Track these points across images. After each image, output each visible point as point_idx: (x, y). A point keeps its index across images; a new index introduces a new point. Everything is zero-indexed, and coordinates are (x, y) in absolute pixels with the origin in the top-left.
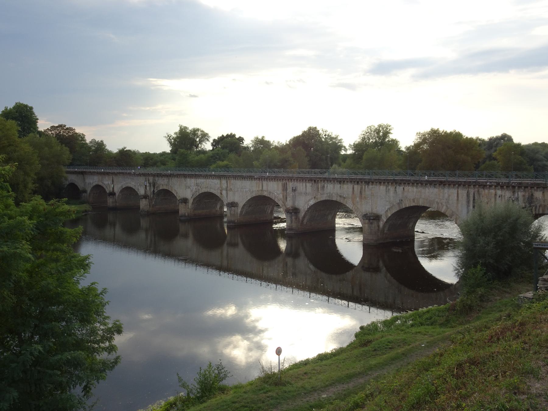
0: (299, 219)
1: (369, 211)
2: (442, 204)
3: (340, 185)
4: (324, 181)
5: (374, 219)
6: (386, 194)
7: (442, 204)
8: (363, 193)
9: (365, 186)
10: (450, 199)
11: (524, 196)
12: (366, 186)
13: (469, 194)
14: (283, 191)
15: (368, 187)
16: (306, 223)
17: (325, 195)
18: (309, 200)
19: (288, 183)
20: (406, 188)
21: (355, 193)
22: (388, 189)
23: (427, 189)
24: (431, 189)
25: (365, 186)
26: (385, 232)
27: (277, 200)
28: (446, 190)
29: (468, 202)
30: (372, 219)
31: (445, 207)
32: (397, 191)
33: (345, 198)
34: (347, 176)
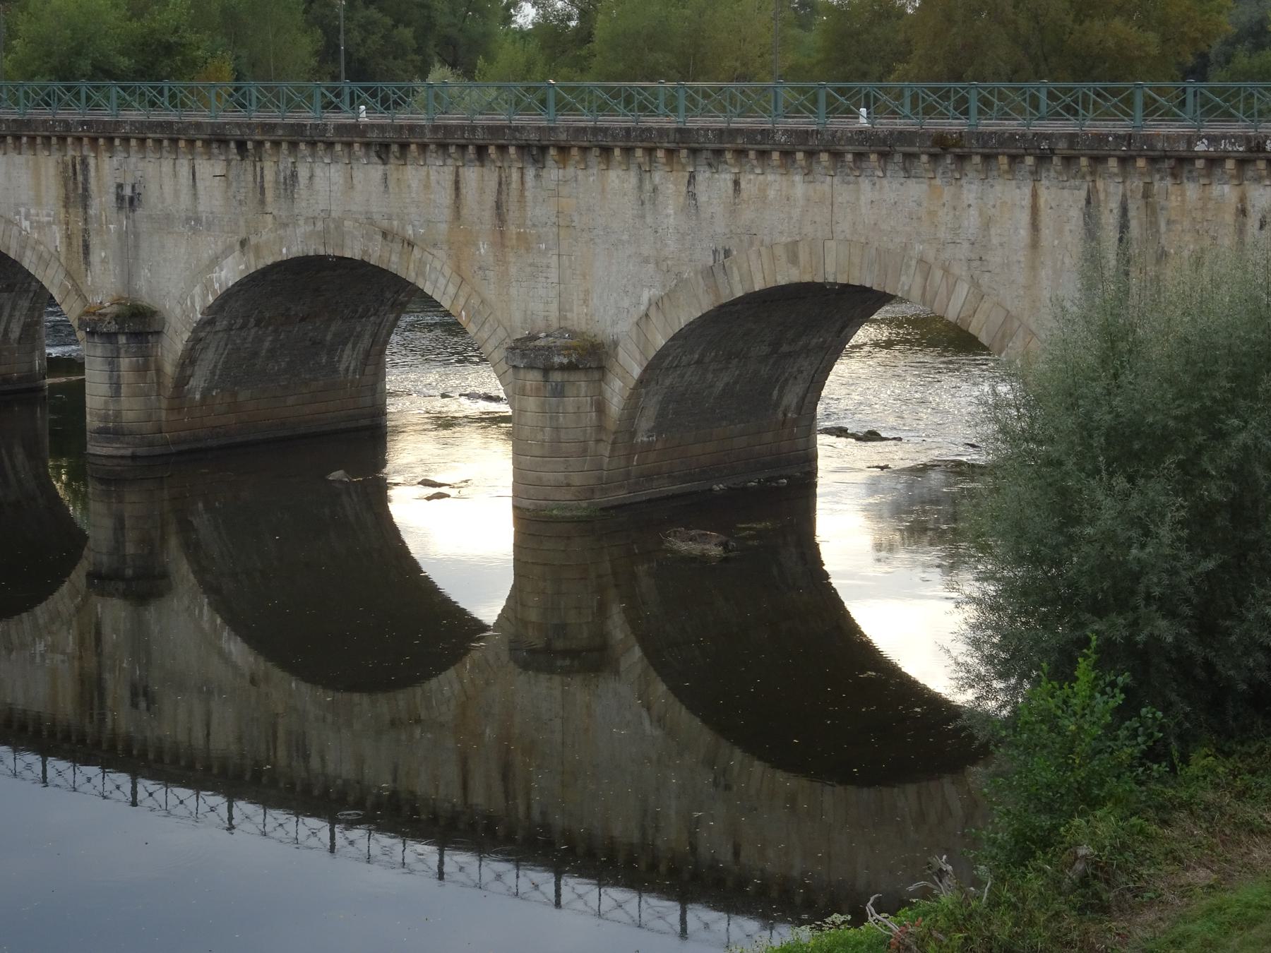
0: (159, 371)
1: (546, 318)
2: (946, 271)
3: (381, 168)
4: (294, 145)
5: (570, 367)
6: (643, 217)
7: (946, 271)
8: (513, 214)
10: (995, 241)
14: (66, 206)
15: (537, 176)
16: (204, 397)
17: (303, 229)
18: (215, 261)
19: (92, 162)
20: (753, 181)
21: (465, 212)
22: (648, 186)
23: (865, 184)
24: (885, 182)
26: (641, 438)
27: (34, 259)
28: (971, 190)
30: (562, 368)
31: (963, 290)
32: (702, 198)
33: (411, 244)
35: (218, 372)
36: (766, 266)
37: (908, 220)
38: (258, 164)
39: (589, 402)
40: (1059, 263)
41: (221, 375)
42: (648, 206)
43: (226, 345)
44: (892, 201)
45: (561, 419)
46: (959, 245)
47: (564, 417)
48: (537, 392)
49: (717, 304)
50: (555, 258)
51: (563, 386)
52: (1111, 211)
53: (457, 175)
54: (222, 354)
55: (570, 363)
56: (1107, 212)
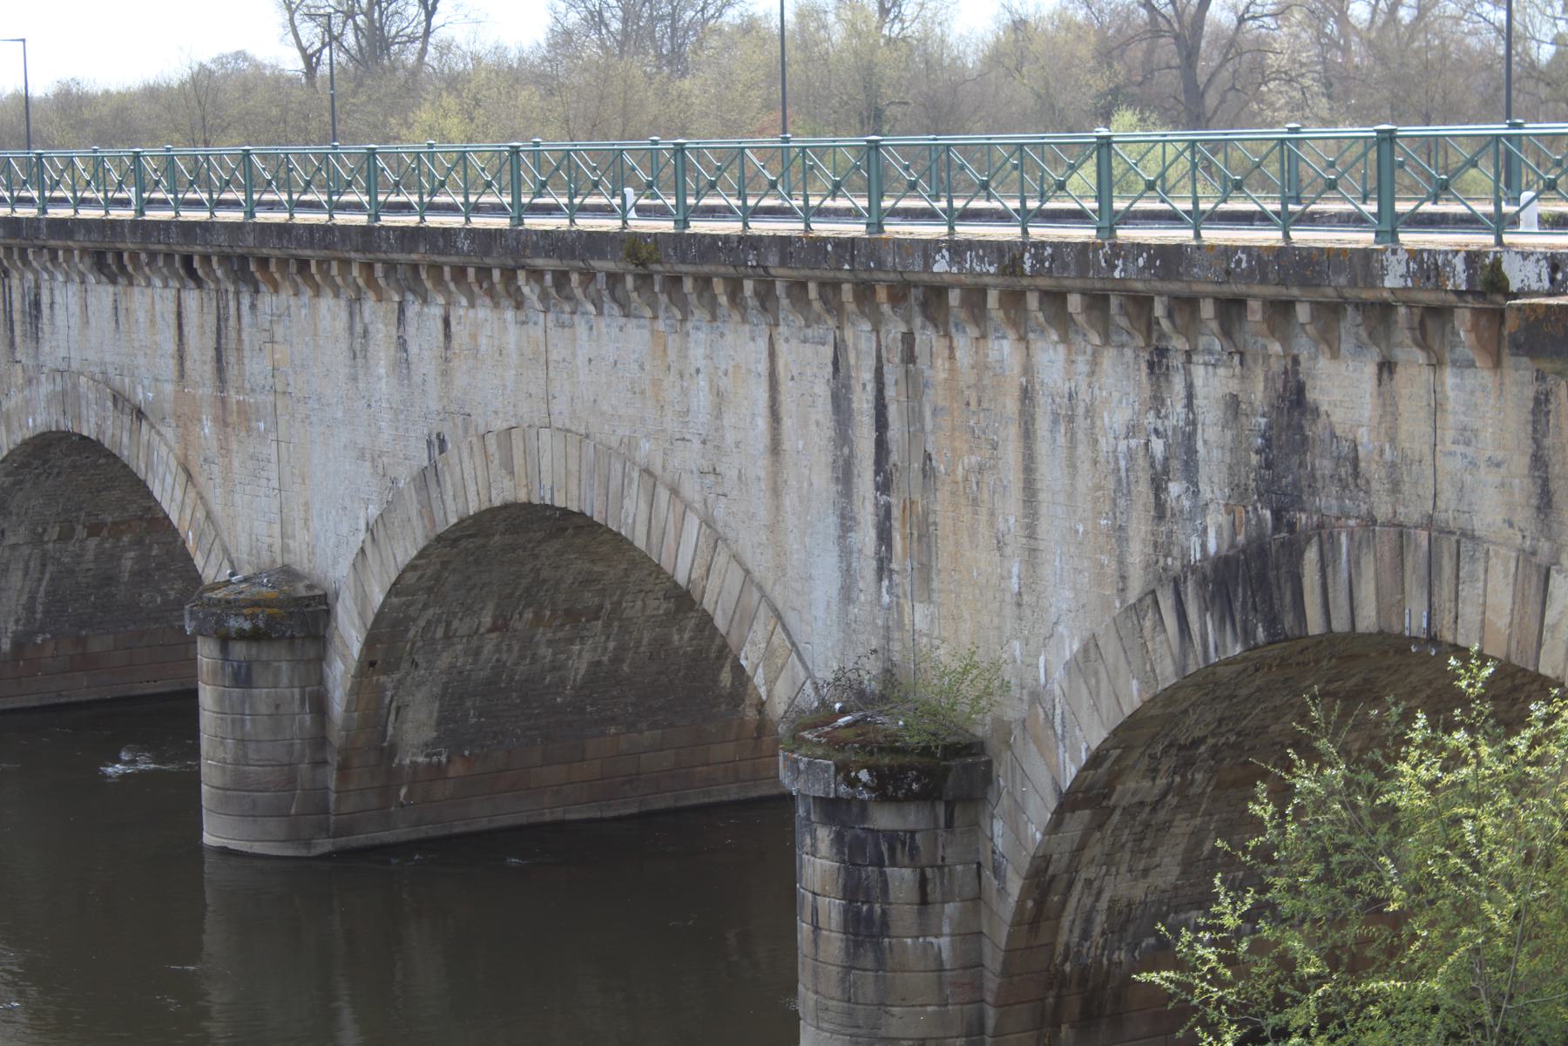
3: (110, 289)
5: (255, 636)
6: (355, 379)
8: (232, 372)
9: (237, 293)
10: (730, 437)
11: (1234, 405)
12: (246, 301)
13: (848, 387)
24: (602, 324)
25: (237, 293)
29: (844, 475)
30: (242, 636)
33: (139, 414)
34: (1357, 220)
35: (40, 608)
36: (479, 473)
37: (630, 395)
38: (6, 281)
39: (297, 696)
40: (805, 484)
41: (46, 612)
42: (360, 361)
43: (44, 566)
44: (612, 360)
45: (248, 725)
46: (688, 444)
47: (253, 721)
49: (432, 536)
50: (274, 444)
51: (249, 669)
52: (864, 386)
53: (179, 298)
54: (40, 580)
55: (255, 628)
56: (858, 388)
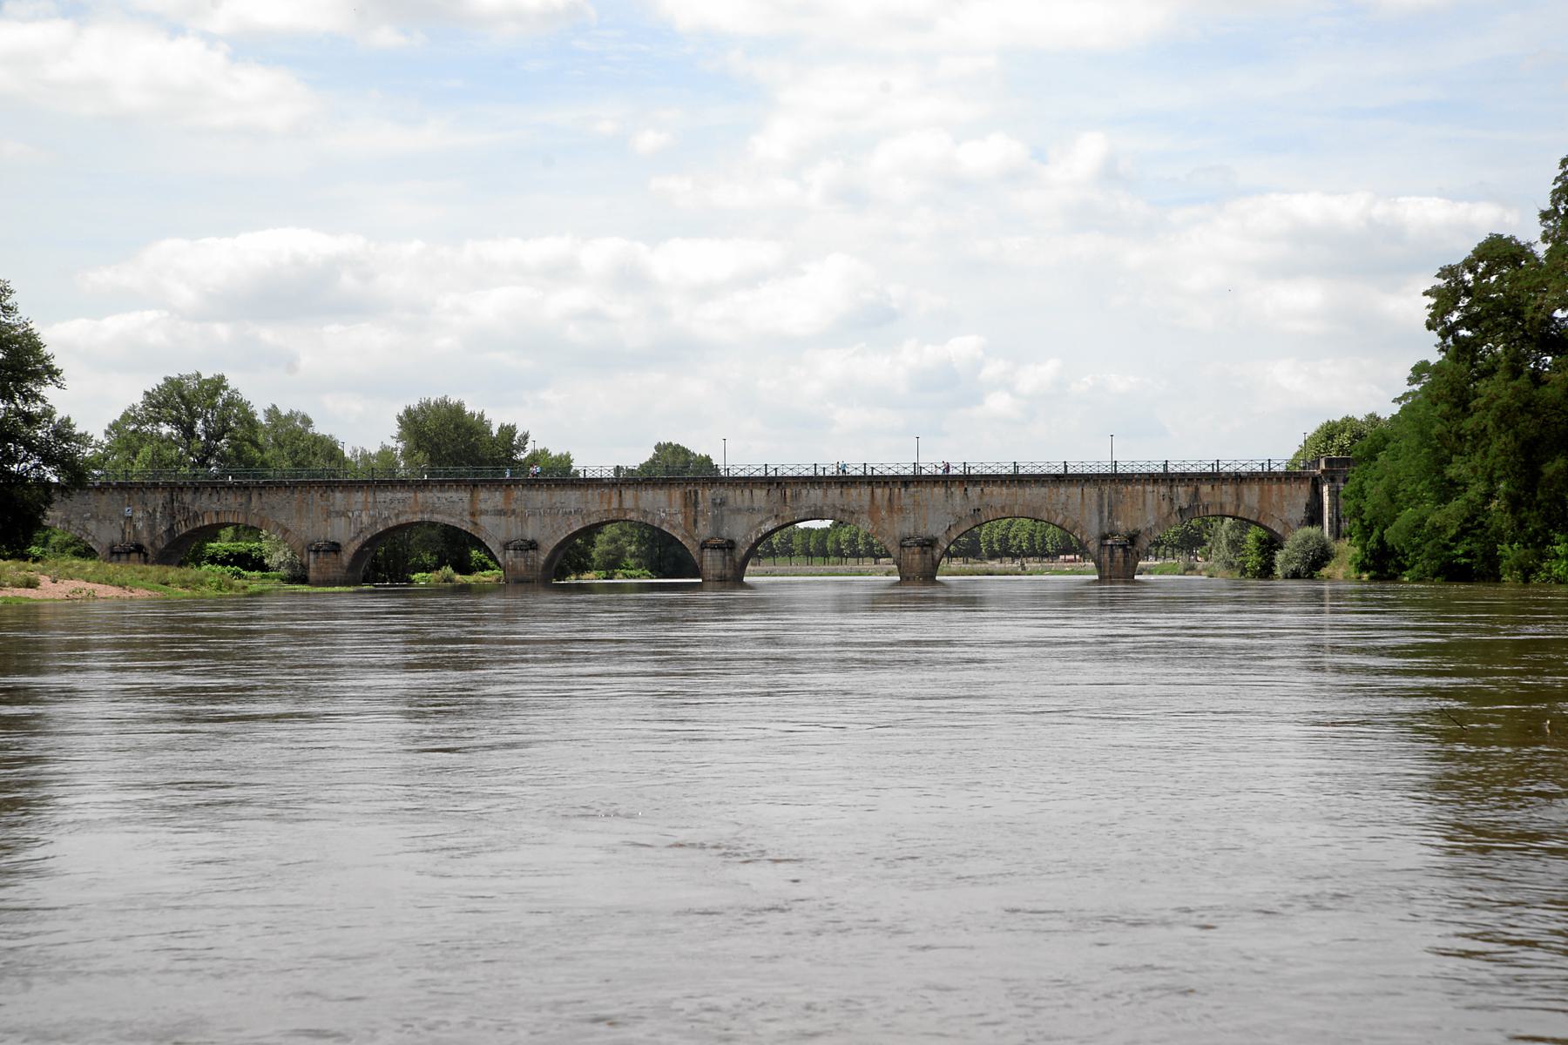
2: (1055, 511)
7: (1055, 511)
11: (1186, 492)
12: (903, 490)
18: (762, 523)
19: (700, 492)
20: (987, 490)
23: (1027, 489)
28: (1062, 490)
31: (1061, 517)
32: (970, 495)
48: (919, 553)
